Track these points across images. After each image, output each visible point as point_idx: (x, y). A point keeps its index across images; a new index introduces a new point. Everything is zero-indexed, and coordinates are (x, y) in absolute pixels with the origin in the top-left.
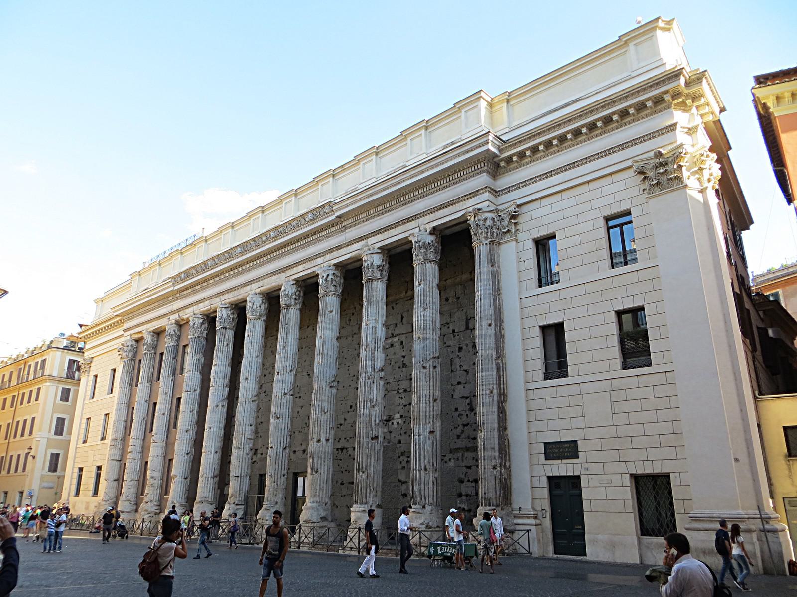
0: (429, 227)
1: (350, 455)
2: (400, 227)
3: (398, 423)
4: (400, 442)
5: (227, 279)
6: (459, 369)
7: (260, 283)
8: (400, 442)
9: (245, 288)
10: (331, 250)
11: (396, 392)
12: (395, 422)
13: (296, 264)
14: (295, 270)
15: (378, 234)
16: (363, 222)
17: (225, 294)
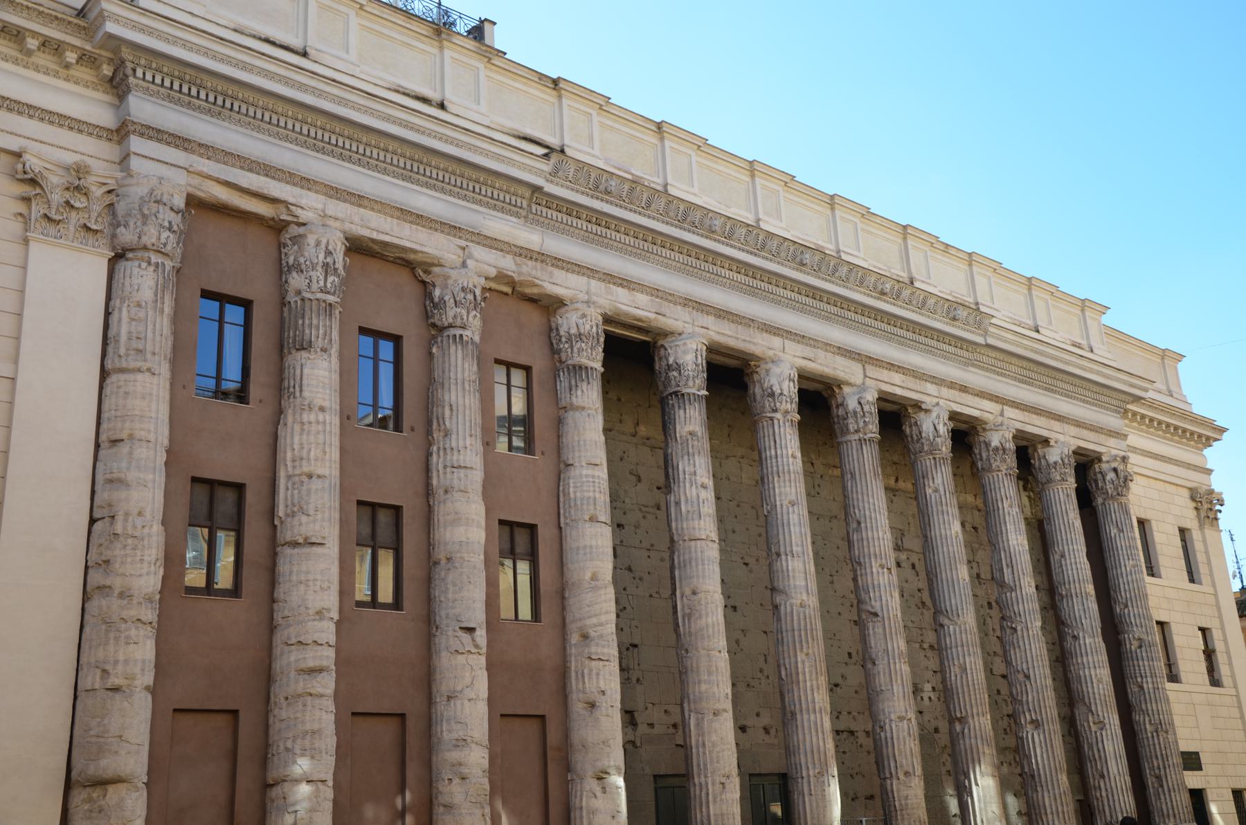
0: (1075, 443)
1: (861, 746)
2: (1042, 418)
3: (930, 698)
4: (936, 730)
5: (714, 280)
6: (992, 633)
7: (809, 352)
8: (936, 730)
9: (765, 335)
10: (952, 385)
11: (917, 646)
12: (926, 699)
13: (891, 366)
14: (885, 375)
15: (1017, 408)
16: (998, 374)
17: (708, 313)
